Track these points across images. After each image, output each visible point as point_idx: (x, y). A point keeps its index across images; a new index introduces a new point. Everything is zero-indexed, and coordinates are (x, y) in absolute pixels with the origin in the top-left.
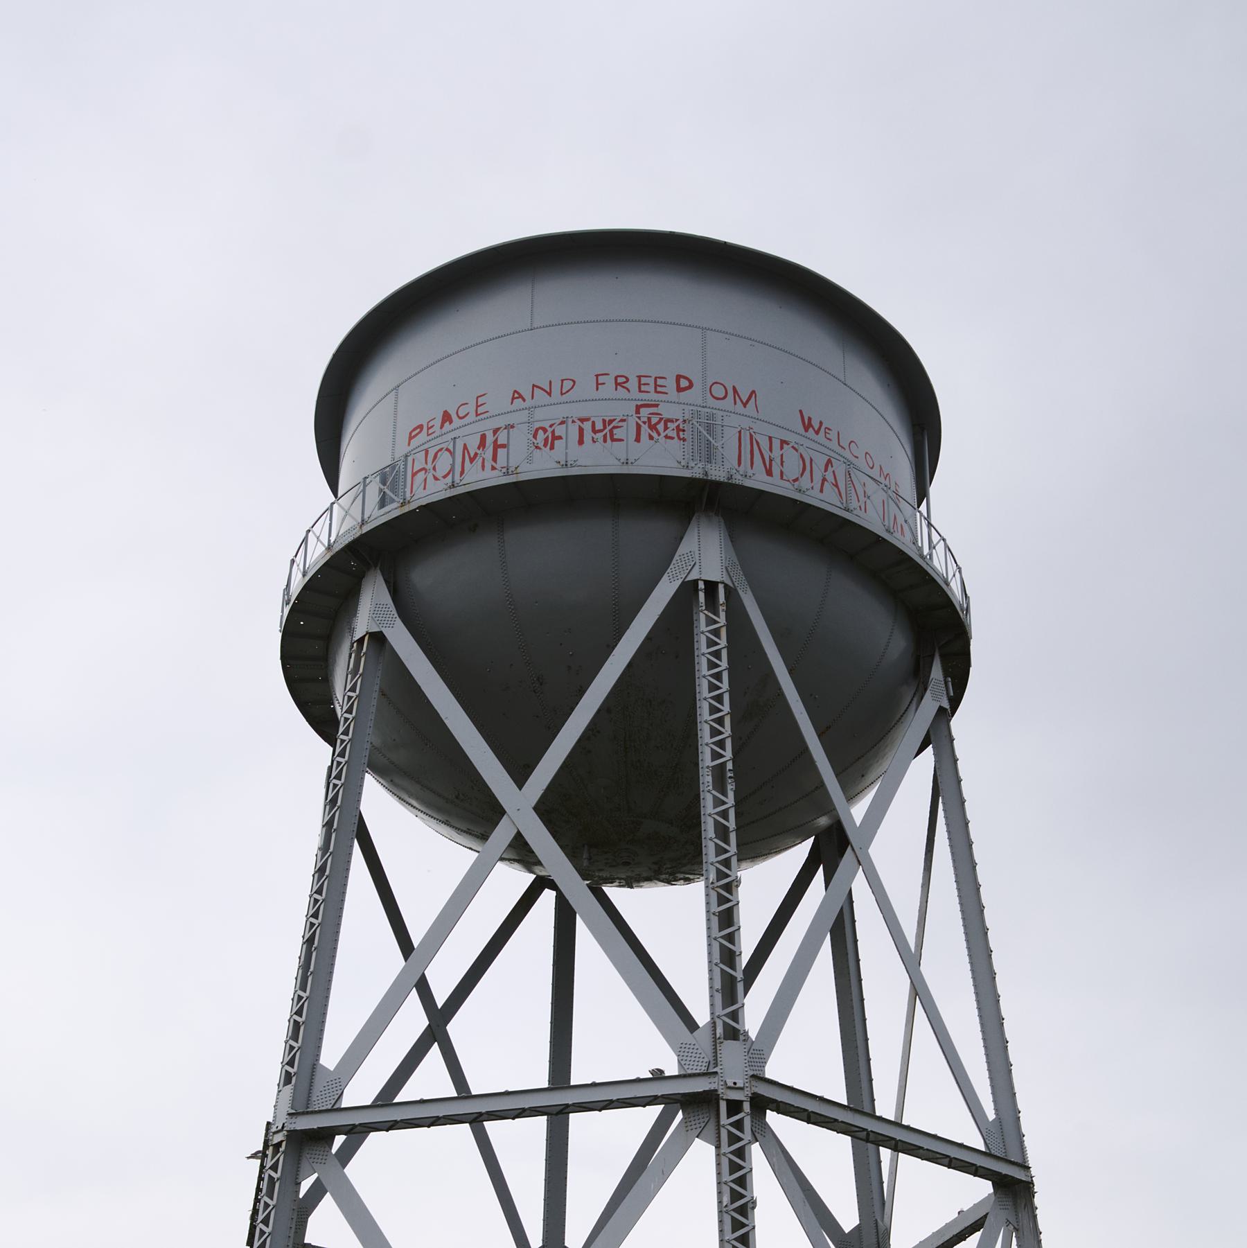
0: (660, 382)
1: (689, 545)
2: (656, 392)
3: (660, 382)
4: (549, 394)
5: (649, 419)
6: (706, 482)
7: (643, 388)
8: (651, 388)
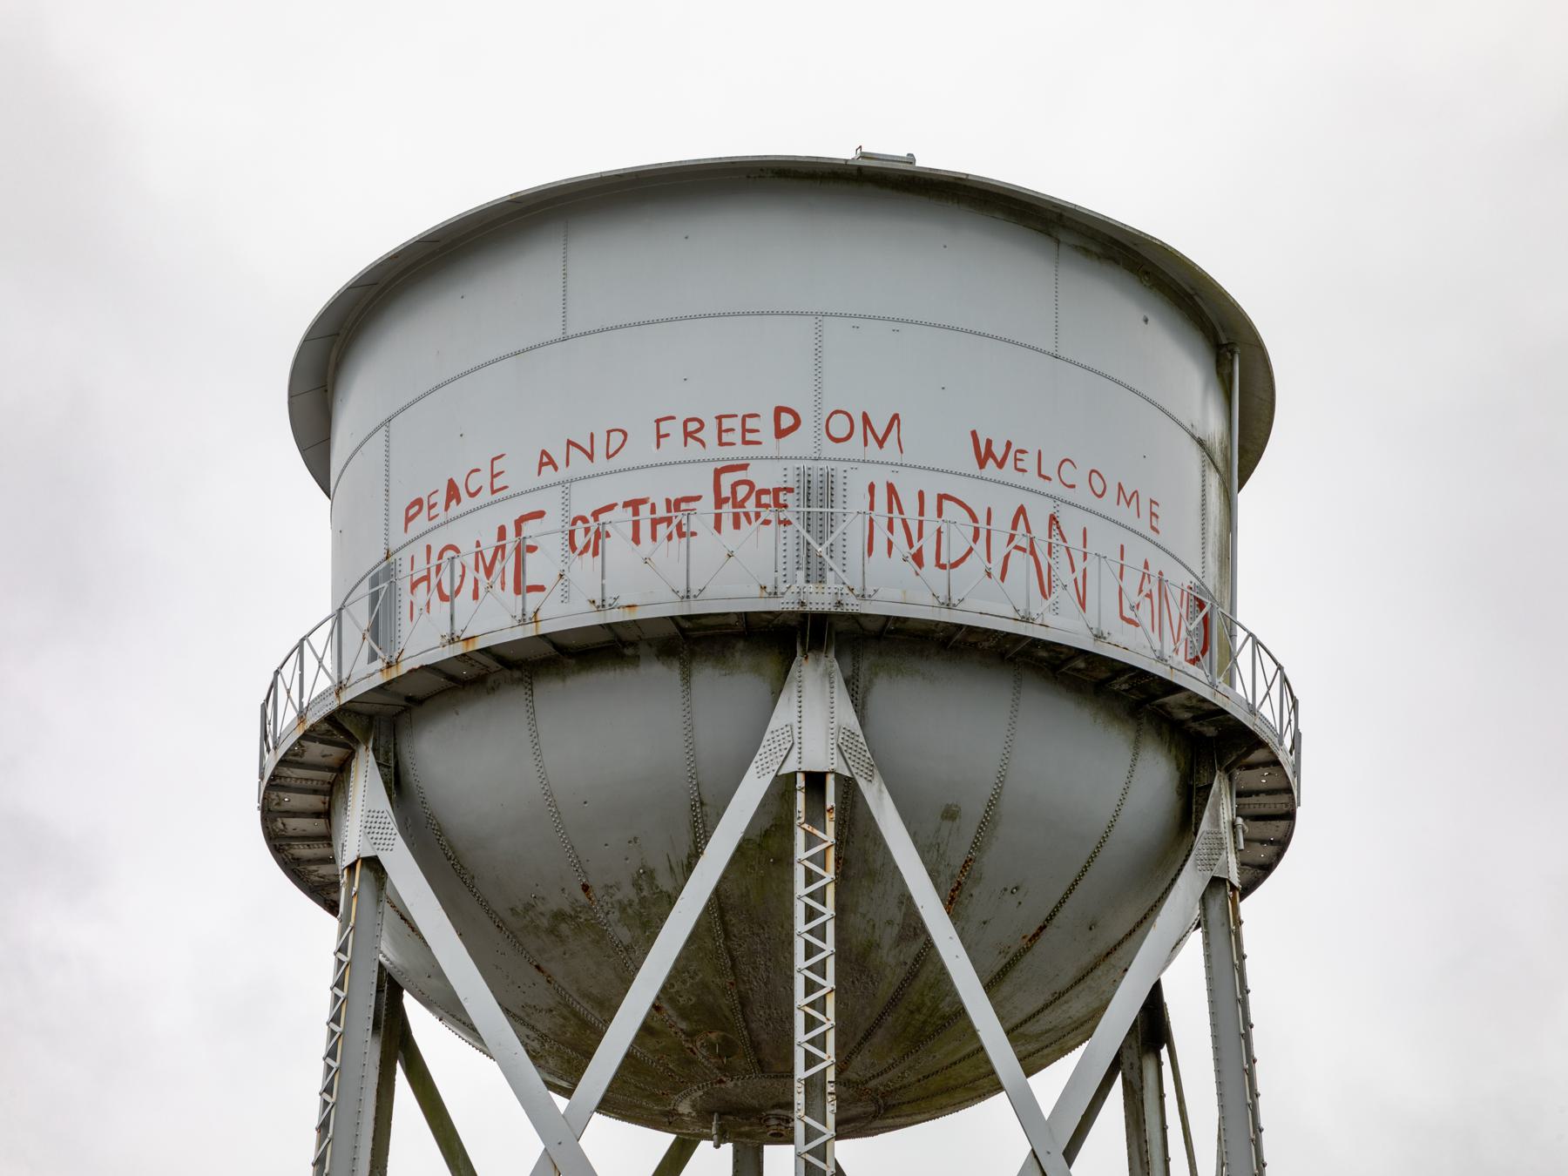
0: (750, 424)
1: (784, 714)
2: (745, 442)
3: (750, 424)
4: (591, 457)
5: (734, 493)
6: (804, 615)
7: (726, 438)
8: (735, 437)
